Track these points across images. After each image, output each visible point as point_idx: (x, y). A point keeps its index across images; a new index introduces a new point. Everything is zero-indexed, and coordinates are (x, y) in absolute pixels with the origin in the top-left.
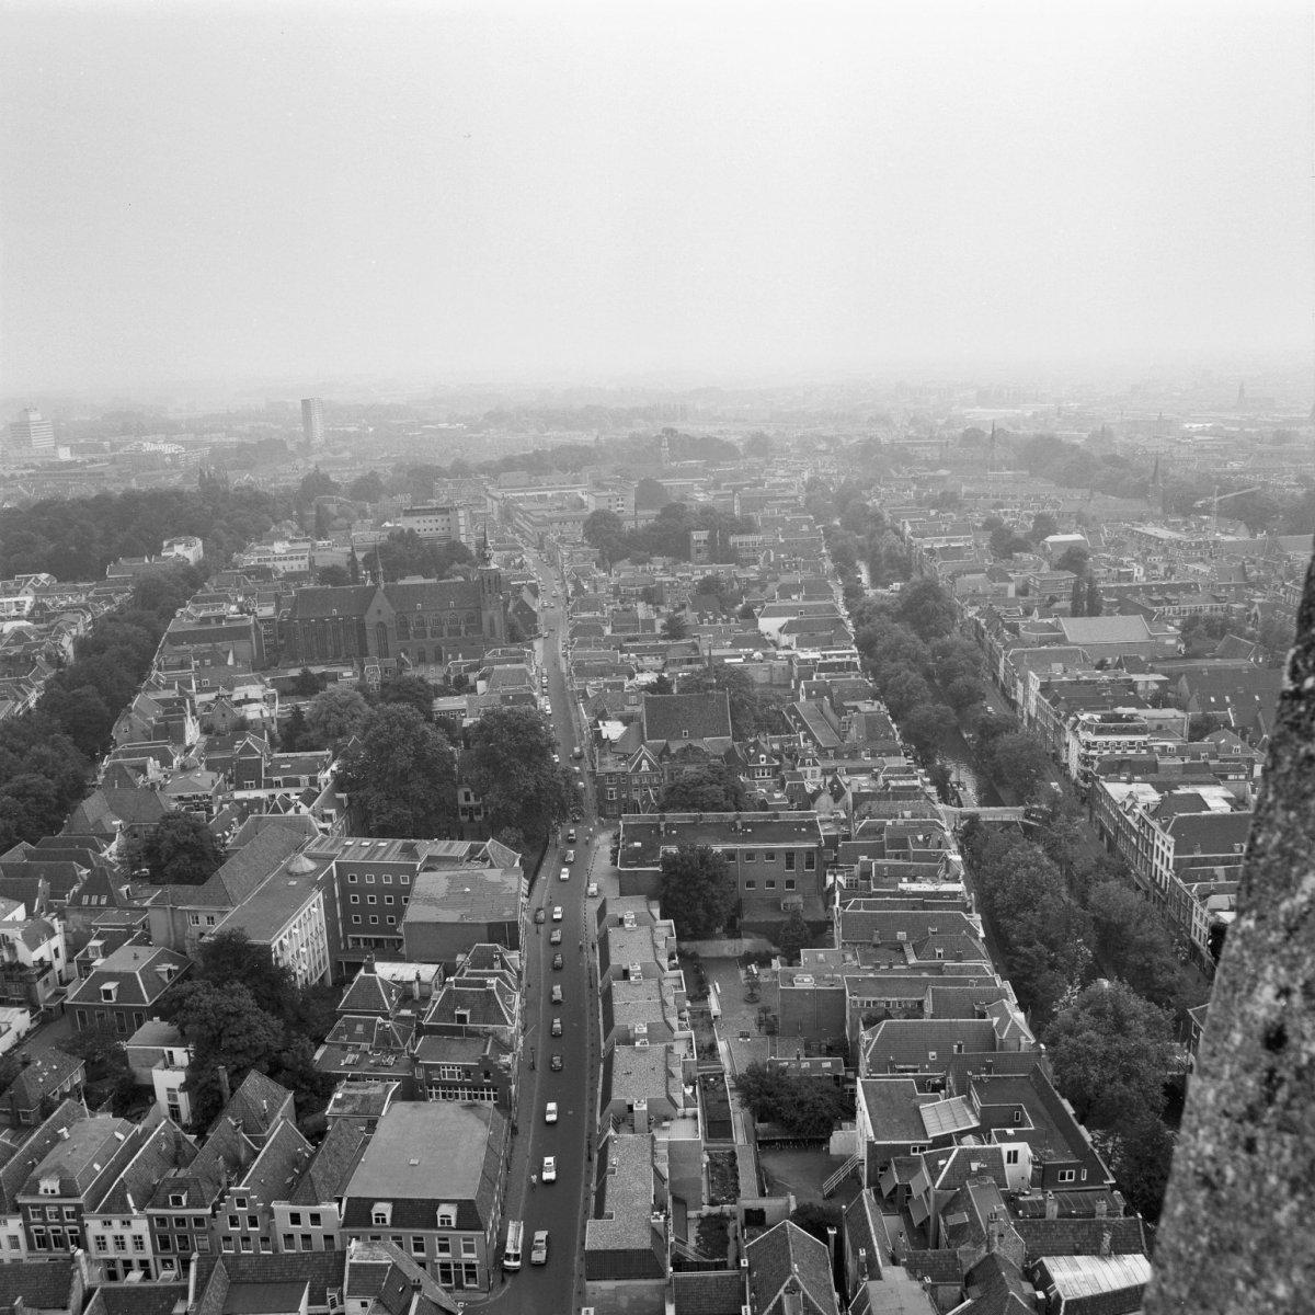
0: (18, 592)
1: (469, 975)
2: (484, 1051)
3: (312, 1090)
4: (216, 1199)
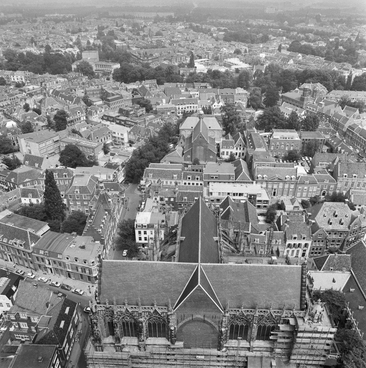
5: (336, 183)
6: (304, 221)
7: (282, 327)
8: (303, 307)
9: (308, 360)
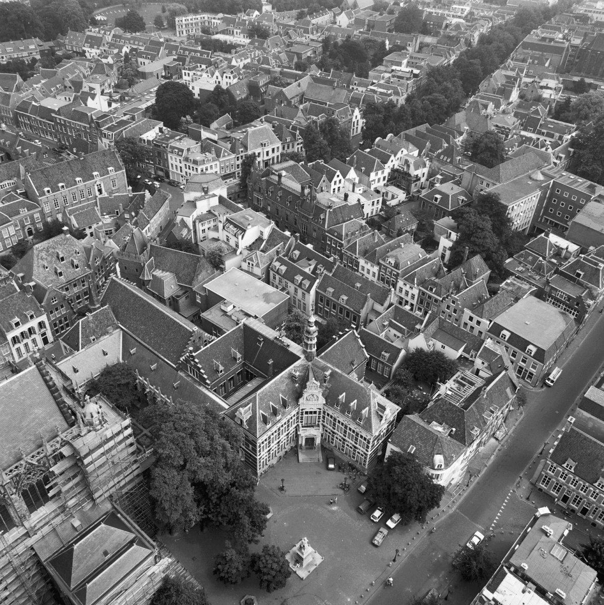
0: (465, 3)
1: (591, 257)
2: (582, 294)
3: (499, 274)
4: (445, 296)
5: (40, 209)
6: (19, 290)
7: (56, 469)
8: (70, 418)
9: (118, 482)
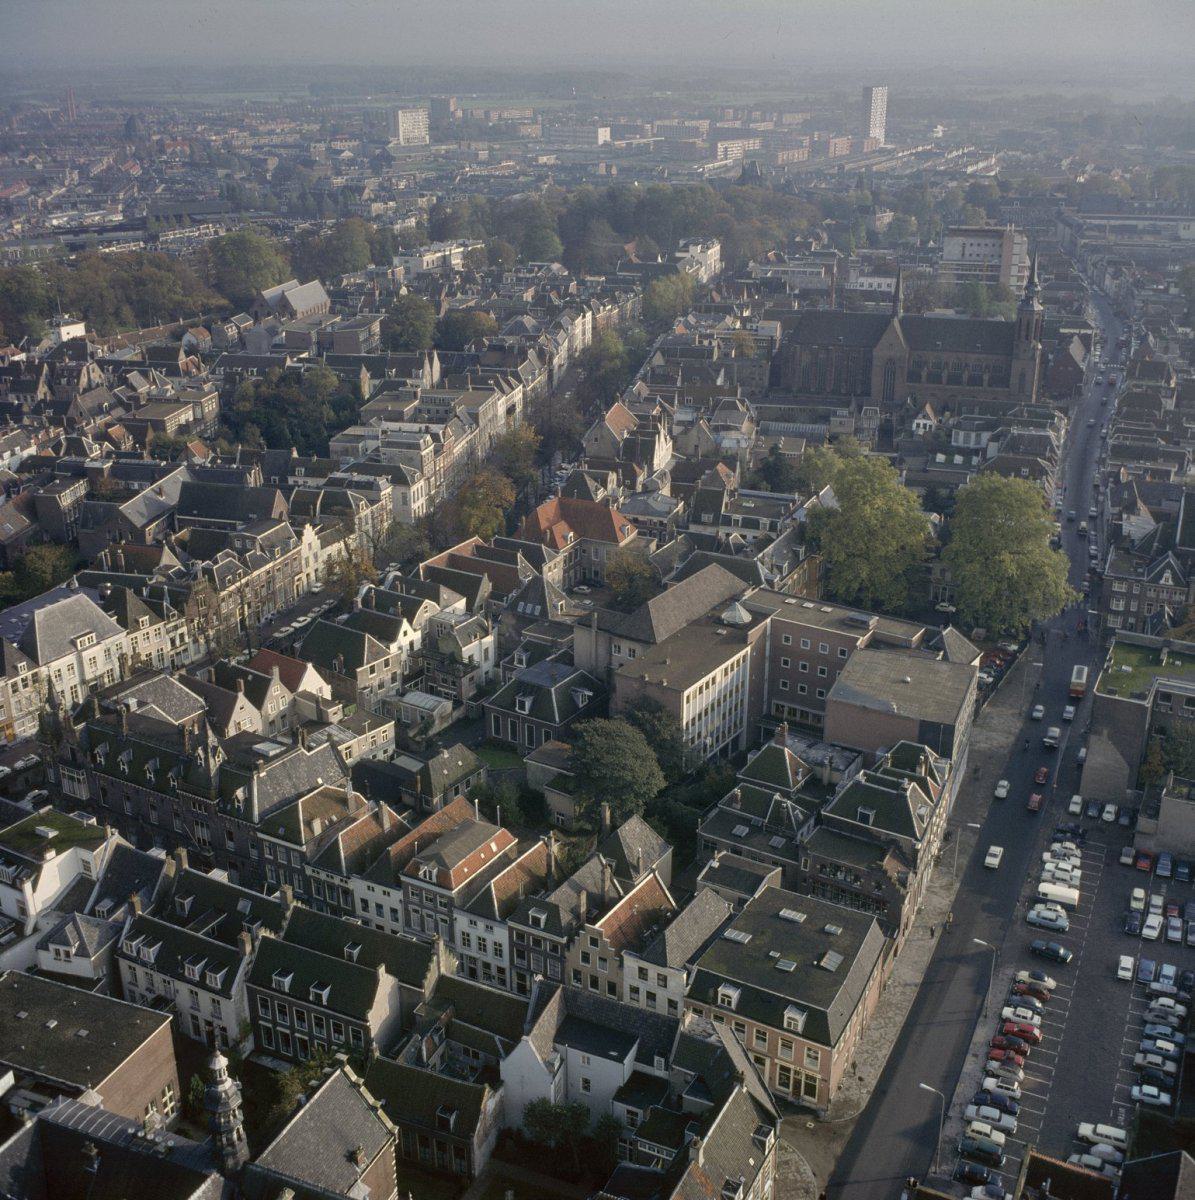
1: (886, 772)
